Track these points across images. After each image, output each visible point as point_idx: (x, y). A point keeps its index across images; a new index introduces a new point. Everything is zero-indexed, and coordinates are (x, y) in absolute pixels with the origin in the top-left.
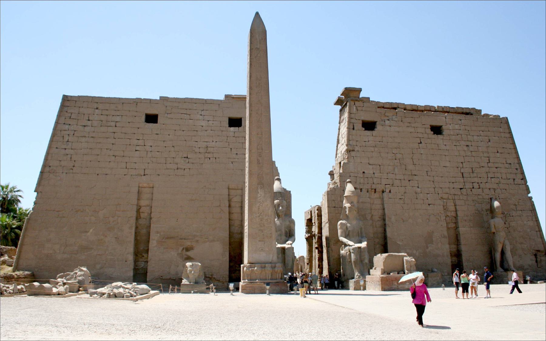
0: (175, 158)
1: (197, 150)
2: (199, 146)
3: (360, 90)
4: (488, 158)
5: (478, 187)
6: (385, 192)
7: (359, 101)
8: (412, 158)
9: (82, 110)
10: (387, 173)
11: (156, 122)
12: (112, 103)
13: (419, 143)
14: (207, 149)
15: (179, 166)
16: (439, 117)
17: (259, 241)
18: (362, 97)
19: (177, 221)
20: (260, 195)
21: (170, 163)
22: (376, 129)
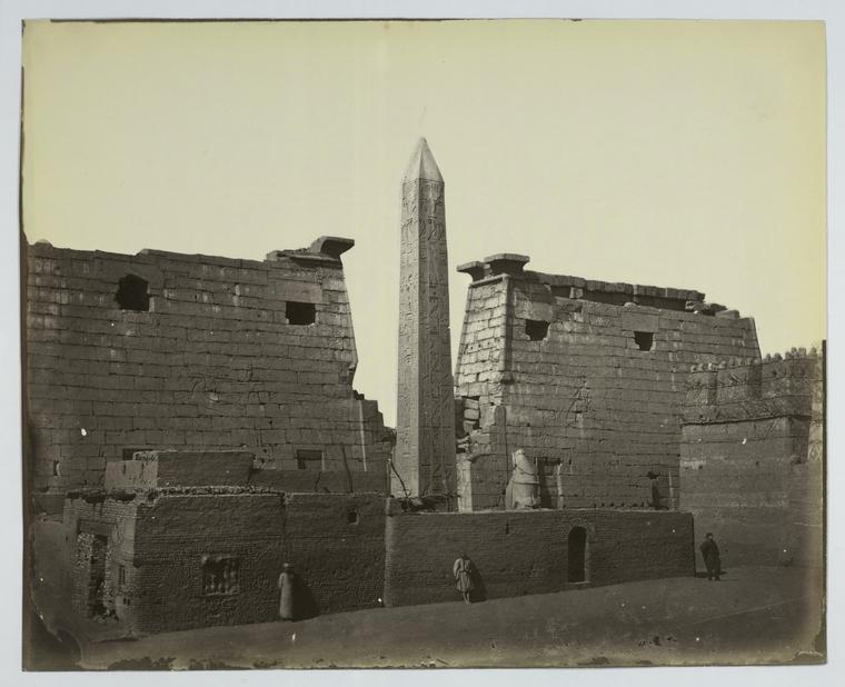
3: (525, 260)
18: (528, 272)
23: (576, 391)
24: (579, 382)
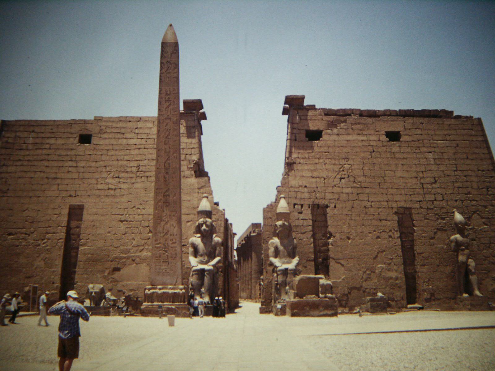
1: (129, 170)
2: (131, 165)
4: (455, 166)
5: (442, 199)
6: (329, 208)
7: (303, 110)
8: (362, 169)
9: (18, 134)
10: (333, 187)
11: (89, 142)
12: (48, 126)
13: (371, 152)
14: (139, 168)
15: (110, 186)
16: (397, 122)
17: (163, 262)
18: (307, 106)
19: (105, 242)
22: (321, 139)
23: (340, 166)
24: (343, 162)
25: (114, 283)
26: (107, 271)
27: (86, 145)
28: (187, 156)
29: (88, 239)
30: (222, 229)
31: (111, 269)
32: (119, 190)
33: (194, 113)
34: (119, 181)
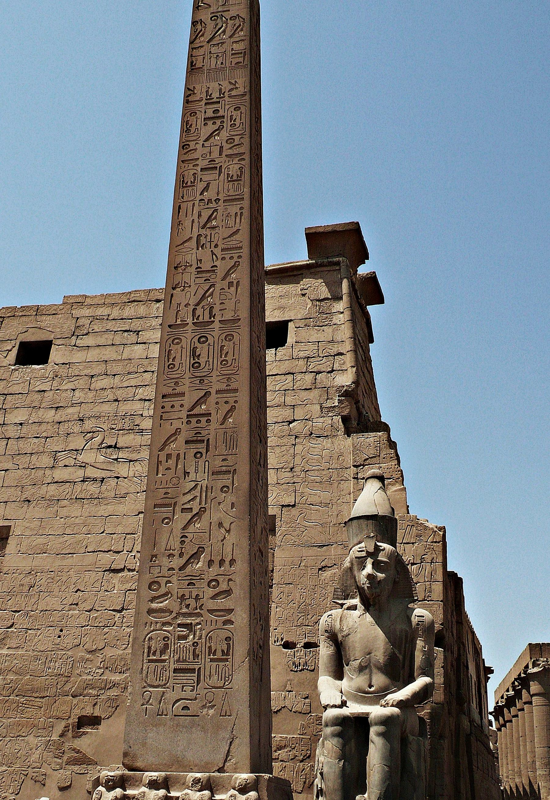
0: (83, 450)
15: (91, 472)
20: (193, 484)
21: (65, 466)
25: (76, 768)
26: (60, 727)
27: (33, 366)
28: (319, 377)
29: (11, 626)
30: (438, 588)
31: (74, 720)
32: (113, 482)
33: (338, 263)
34: (115, 457)
